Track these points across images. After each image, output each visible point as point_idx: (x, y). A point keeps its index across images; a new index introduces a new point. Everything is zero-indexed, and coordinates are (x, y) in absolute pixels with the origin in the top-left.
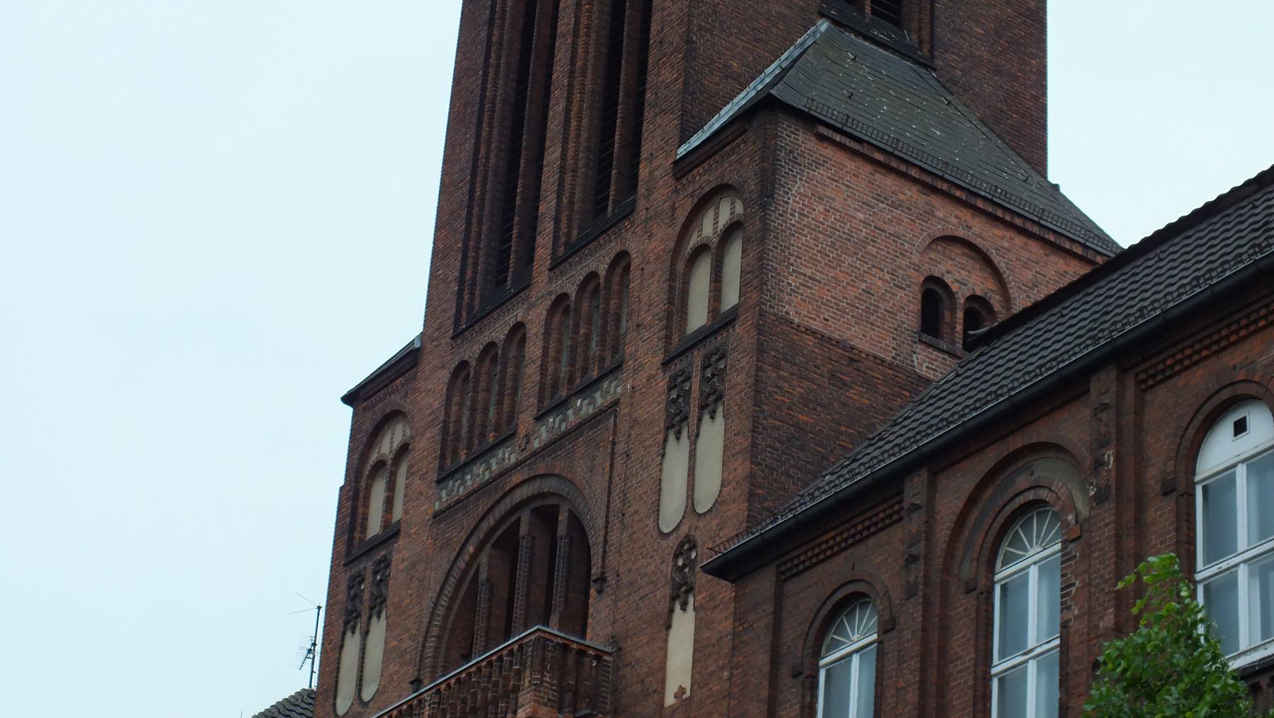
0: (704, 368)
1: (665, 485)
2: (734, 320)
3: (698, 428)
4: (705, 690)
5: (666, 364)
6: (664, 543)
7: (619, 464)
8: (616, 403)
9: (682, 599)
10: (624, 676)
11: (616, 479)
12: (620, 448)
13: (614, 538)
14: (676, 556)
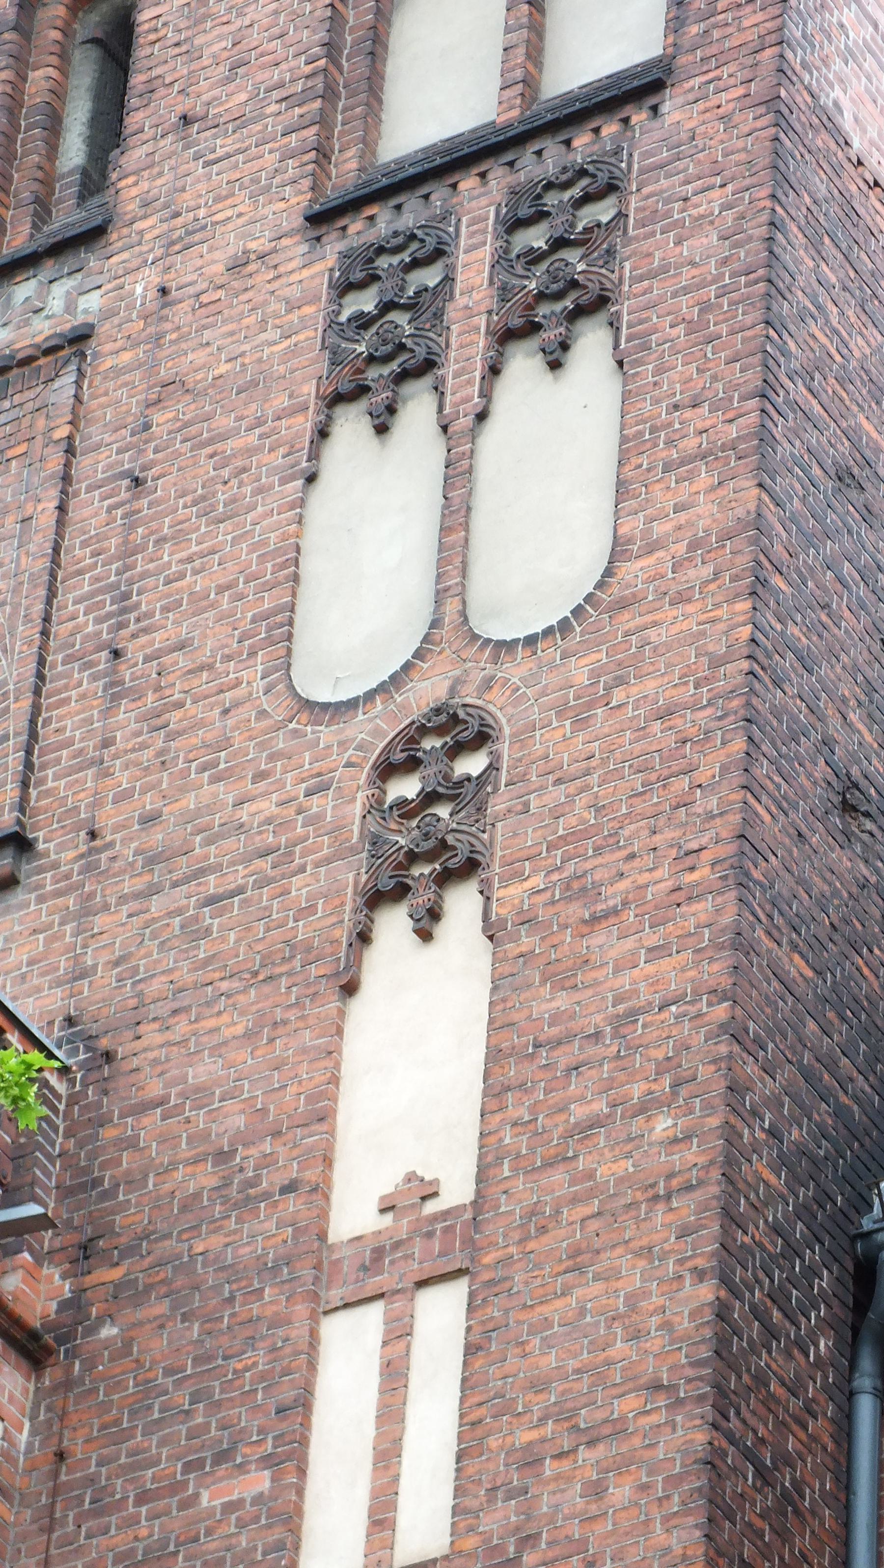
0: (515, 224)
1: (312, 566)
2: (656, 86)
3: (486, 394)
4: (558, 1176)
5: (321, 219)
6: (326, 734)
7: (91, 510)
8: (80, 338)
9: (422, 897)
10: (132, 1143)
11: (76, 551)
12: (92, 466)
13: (71, 721)
14: (387, 770)
